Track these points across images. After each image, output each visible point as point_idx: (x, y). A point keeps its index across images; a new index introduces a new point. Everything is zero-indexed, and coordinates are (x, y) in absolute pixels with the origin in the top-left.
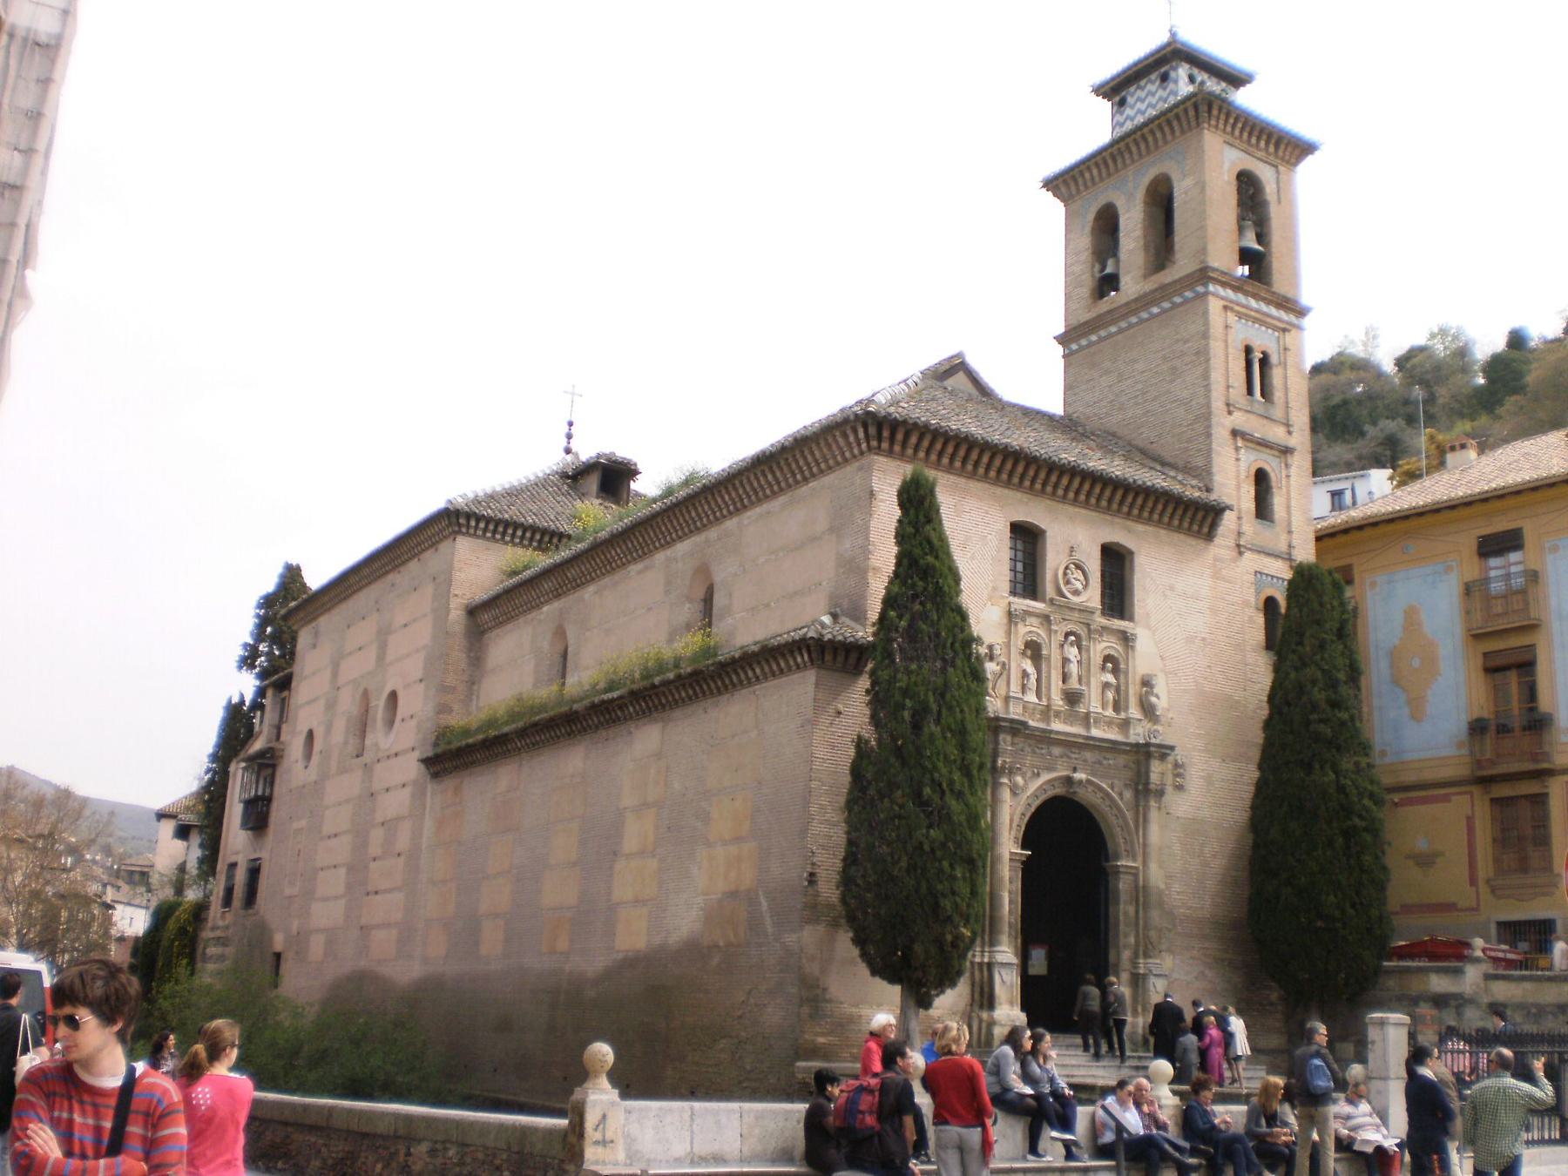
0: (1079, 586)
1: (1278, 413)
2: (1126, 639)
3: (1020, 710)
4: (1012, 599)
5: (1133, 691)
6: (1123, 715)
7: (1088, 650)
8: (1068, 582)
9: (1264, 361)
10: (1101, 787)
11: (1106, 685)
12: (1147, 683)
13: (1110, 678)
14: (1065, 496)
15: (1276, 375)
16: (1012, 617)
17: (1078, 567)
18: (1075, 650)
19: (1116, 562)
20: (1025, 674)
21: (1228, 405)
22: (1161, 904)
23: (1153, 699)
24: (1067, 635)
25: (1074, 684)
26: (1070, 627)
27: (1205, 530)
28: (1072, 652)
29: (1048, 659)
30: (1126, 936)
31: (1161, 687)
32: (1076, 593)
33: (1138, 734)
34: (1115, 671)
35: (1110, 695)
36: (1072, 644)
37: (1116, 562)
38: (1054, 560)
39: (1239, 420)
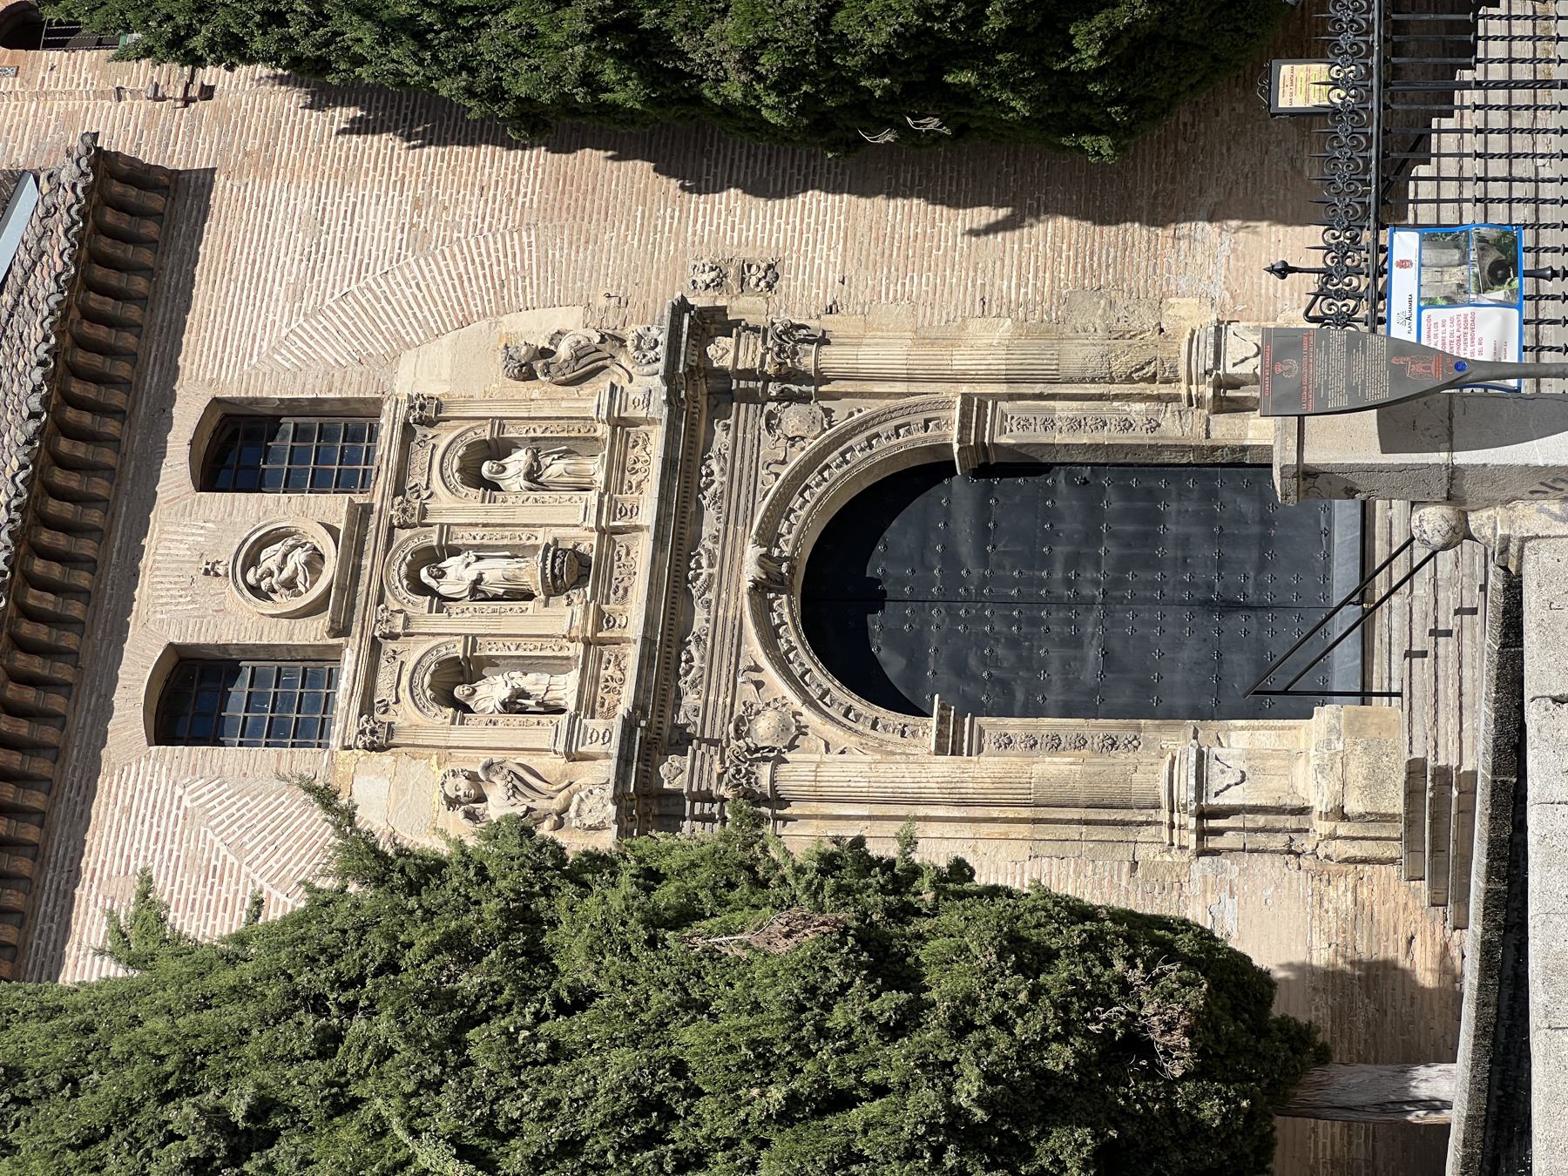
0: (299, 557)
2: (426, 414)
3: (597, 725)
4: (335, 742)
5: (545, 401)
6: (603, 431)
7: (445, 529)
8: (290, 584)
10: (773, 467)
11: (532, 475)
12: (531, 365)
13: (518, 461)
14: (91, 565)
17: (252, 560)
18: (452, 564)
19: (241, 448)
20: (514, 704)
22: (1051, 331)
23: (564, 351)
24: (419, 588)
25: (530, 573)
27: (155, 201)
28: (457, 575)
29: (472, 640)
30: (1127, 425)
31: (532, 328)
32: (315, 560)
33: (643, 386)
34: (498, 449)
35: (555, 469)
37: (241, 448)
38: (235, 621)
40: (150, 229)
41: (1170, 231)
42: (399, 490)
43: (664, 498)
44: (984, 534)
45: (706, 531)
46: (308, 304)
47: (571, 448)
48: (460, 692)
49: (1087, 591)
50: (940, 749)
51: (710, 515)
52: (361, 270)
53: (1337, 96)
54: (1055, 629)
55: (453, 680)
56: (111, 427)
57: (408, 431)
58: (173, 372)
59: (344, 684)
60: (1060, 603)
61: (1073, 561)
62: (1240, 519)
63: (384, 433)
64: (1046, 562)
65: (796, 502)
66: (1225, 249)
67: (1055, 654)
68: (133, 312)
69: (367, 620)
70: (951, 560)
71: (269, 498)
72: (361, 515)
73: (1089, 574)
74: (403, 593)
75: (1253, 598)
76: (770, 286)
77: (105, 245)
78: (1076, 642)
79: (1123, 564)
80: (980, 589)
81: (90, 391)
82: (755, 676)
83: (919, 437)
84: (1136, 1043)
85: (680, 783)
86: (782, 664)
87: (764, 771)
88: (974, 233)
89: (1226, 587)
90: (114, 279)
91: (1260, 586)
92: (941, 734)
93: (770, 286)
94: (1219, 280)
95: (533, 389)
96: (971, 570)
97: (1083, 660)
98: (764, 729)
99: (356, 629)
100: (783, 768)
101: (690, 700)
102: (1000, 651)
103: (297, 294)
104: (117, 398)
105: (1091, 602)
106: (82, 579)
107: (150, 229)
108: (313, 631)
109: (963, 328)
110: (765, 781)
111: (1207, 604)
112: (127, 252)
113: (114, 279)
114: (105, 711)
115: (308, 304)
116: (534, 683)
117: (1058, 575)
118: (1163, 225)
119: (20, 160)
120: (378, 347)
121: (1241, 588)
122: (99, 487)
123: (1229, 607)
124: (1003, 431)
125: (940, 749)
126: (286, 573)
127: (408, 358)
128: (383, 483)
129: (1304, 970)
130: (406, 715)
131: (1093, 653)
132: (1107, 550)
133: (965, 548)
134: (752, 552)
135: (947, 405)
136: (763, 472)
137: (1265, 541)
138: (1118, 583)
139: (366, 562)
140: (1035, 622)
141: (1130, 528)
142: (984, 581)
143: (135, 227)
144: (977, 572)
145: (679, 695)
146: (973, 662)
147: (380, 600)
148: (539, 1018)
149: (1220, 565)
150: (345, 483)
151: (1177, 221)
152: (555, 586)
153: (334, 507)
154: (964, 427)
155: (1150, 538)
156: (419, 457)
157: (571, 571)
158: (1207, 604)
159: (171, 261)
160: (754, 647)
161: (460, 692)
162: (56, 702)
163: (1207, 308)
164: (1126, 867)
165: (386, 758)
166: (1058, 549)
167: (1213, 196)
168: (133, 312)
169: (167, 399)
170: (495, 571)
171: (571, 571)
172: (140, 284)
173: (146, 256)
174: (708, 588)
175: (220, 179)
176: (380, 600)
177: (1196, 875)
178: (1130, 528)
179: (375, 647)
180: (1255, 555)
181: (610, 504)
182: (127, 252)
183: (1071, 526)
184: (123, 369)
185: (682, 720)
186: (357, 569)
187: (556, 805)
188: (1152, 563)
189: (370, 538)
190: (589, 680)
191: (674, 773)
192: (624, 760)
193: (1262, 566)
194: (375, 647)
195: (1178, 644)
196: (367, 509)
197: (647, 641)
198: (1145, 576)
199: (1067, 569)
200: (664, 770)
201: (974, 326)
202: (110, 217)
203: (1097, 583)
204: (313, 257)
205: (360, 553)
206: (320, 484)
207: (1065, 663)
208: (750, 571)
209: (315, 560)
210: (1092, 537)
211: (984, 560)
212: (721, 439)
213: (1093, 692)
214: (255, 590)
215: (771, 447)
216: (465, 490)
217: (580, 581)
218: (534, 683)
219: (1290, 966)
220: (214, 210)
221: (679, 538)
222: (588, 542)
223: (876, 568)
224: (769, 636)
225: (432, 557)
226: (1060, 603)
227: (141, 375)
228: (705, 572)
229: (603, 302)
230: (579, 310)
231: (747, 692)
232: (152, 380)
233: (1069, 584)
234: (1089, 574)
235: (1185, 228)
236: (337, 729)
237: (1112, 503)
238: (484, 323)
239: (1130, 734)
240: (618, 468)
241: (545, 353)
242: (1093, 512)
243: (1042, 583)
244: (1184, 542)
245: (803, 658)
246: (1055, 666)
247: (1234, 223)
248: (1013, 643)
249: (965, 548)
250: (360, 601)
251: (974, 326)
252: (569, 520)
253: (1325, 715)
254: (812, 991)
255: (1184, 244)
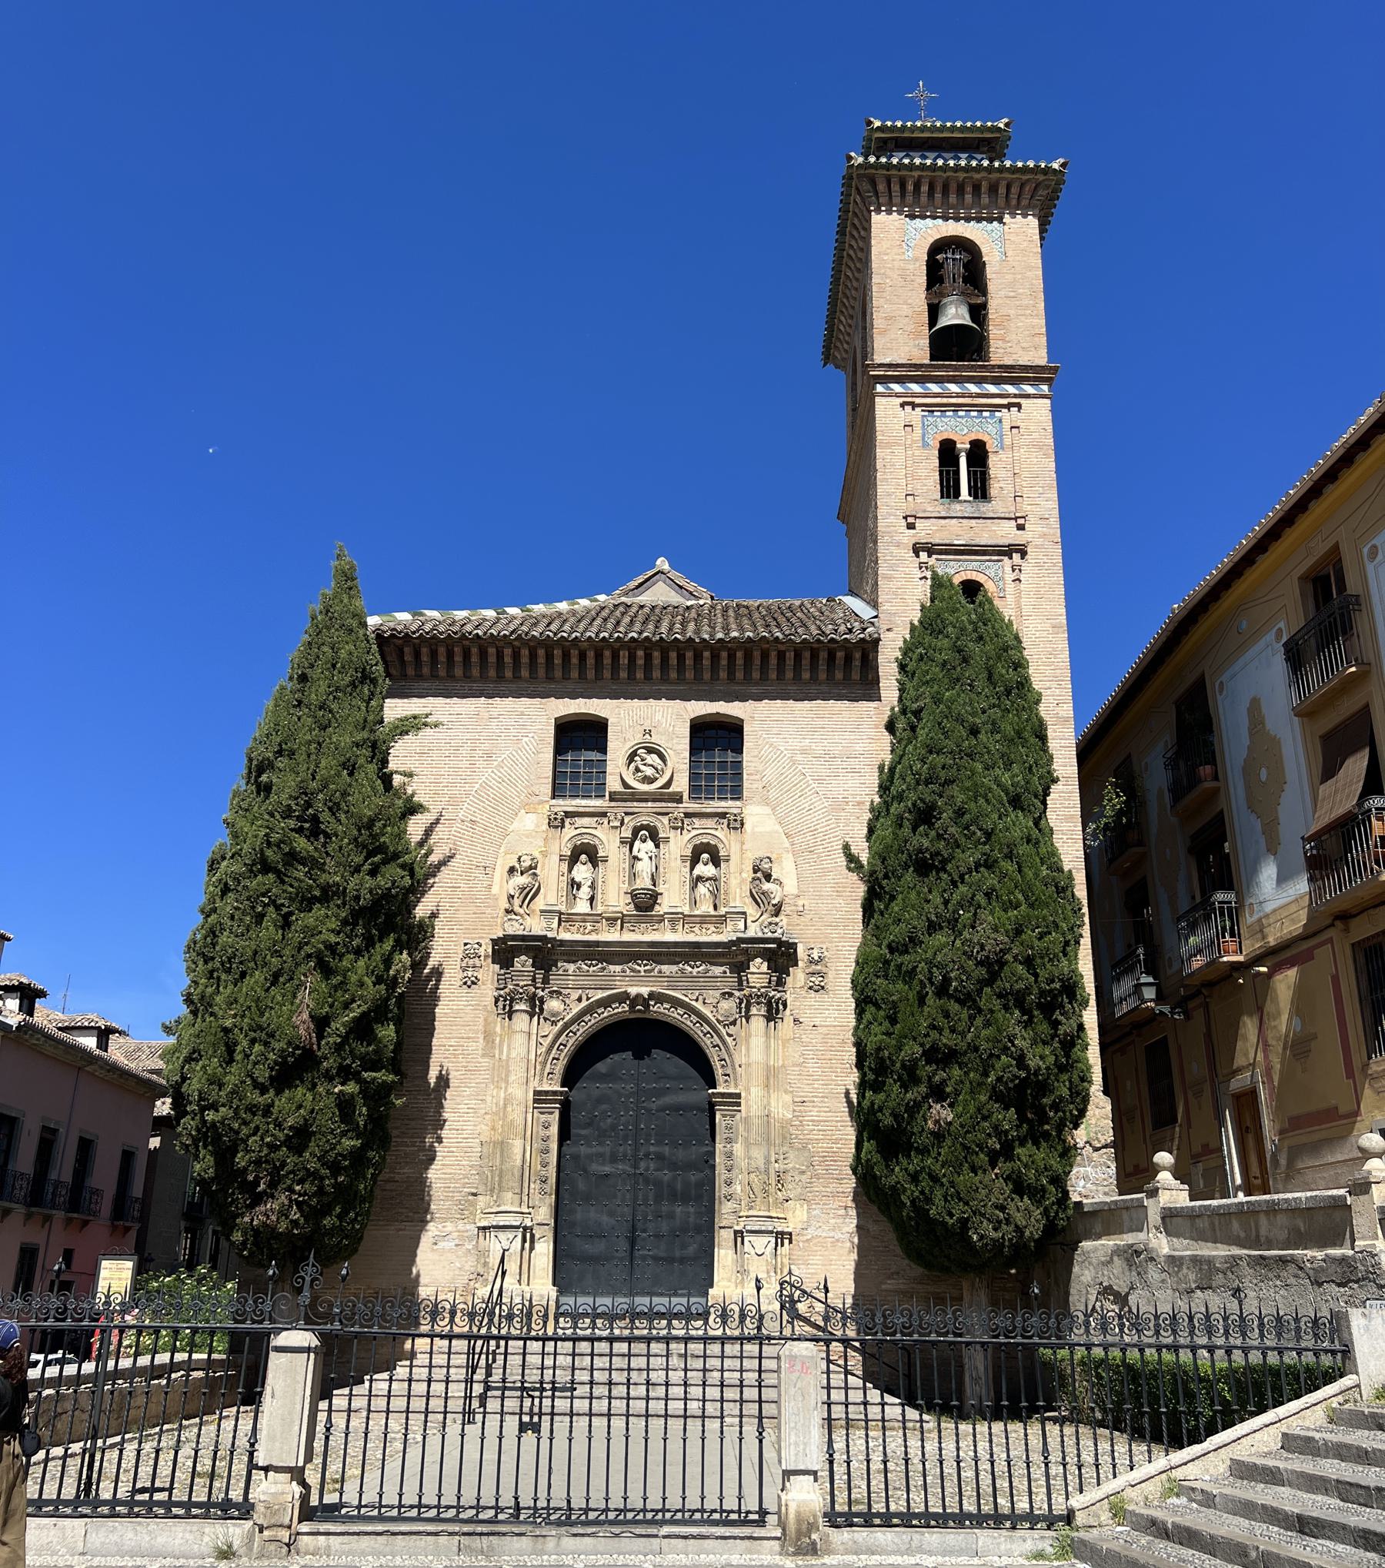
0: (649, 772)
1: (999, 504)
2: (737, 824)
8: (637, 770)
9: (978, 453)
13: (709, 870)
15: (997, 466)
16: (557, 823)
17: (650, 751)
18: (650, 844)
21: (905, 518)
24: (636, 831)
26: (644, 820)
27: (856, 675)
30: (729, 1183)
31: (785, 870)
32: (650, 780)
34: (716, 861)
36: (644, 841)
39: (926, 531)
40: (839, 675)
41: (851, 1204)
42: (687, 815)
43: (676, 944)
44: (676, 1108)
45: (665, 968)
46: (799, 757)
47: (715, 895)
48: (583, 857)
49: (642, 1165)
50: (536, 1093)
51: (674, 968)
52: (819, 780)
53: (101, 1297)
54: (621, 1149)
55: (586, 852)
56: (723, 675)
57: (723, 815)
58: (758, 698)
59: (584, 802)
60: (636, 1150)
61: (660, 1157)
62: (684, 1247)
63: (723, 804)
64: (659, 1143)
65: (681, 1011)
66: (838, 1235)
67: (607, 1149)
68: (789, 675)
69: (619, 808)
70: (660, 1093)
71: (687, 754)
72: (677, 798)
73: (652, 1166)
74: (632, 824)
75: (637, 1254)
76: (811, 988)
77: (823, 655)
78: (614, 1159)
79: (658, 1184)
80: (644, 1108)
81: (740, 661)
82: (584, 997)
83: (719, 1072)
84: (258, 1199)
85: (517, 966)
86: (589, 1010)
87: (523, 1006)
88: (847, 1093)
89: (644, 1239)
90: (806, 662)
91: (644, 1258)
92: (547, 1093)
93: (811, 988)
94: (819, 1232)
95: (748, 875)
96: (655, 1104)
97: (603, 1164)
98: (553, 1005)
99: (613, 804)
100: (526, 1017)
101: (571, 967)
102: (609, 1120)
103: (803, 752)
104: (739, 675)
105: (636, 1167)
106: (640, 675)
107: (839, 675)
108: (613, 784)
109: (786, 1092)
110: (517, 1007)
111: (634, 1229)
112: (822, 666)
113: (806, 662)
114: (573, 696)
115: (799, 757)
116: (585, 892)
117: (652, 1149)
118: (854, 1200)
119: (885, 607)
120: (773, 794)
121: (643, 1248)
122: (690, 675)
123: (633, 1242)
124: (724, 1116)
125: (536, 1093)
126: (642, 768)
127: (768, 810)
128: (694, 807)
129: (416, 1282)
130: (569, 832)
131: (607, 1169)
132: (666, 1175)
133: (668, 1100)
134: (644, 991)
135: (736, 1086)
136: (697, 993)
137: (670, 1260)
138: (647, 1181)
139: (650, 804)
140: (626, 1138)
141: (679, 1187)
142: (649, 1110)
143: (836, 667)
144: (654, 1106)
145: (574, 962)
146: (604, 1107)
147: (627, 814)
148: (278, 908)
149: (656, 1236)
150: (695, 790)
151: (857, 1208)
152: (634, 895)
153: (681, 784)
154: (723, 1095)
155: (674, 1196)
156: (710, 823)
157: (645, 903)
158: (634, 1229)
159: (824, 688)
160: (600, 995)
161: (583, 857)
162: (690, 675)
163: (800, 1226)
164: (474, 1191)
165: (545, 827)
166: (667, 1148)
167: (874, 1228)
168: (789, 675)
169: (743, 698)
170: (644, 867)
171: (645, 903)
172: (806, 675)
173: (823, 676)
174: (633, 970)
175: (875, 704)
176: (627, 814)
177: (468, 1227)
178: (679, 1187)
179: (604, 815)
180: (662, 1254)
181: (685, 918)
182: (822, 666)
183: (681, 1154)
184: (756, 675)
185: (559, 964)
186: (646, 801)
187: (517, 909)
188: (658, 1199)
189: (664, 804)
190: (584, 918)
191: (523, 963)
192: (523, 938)
193: (656, 1258)
194: (604, 815)
195: (611, 1214)
196: (680, 800)
197: (597, 943)
198: (651, 1195)
199: (655, 1153)
200: (523, 958)
201: (788, 1098)
202: (840, 654)
203: (647, 1169)
204: (828, 757)
205: (654, 800)
206: (693, 776)
207: (601, 1155)
208: (633, 991)
209: (650, 780)
210: (674, 1166)
211: (662, 1109)
212: (717, 970)
213: (585, 1171)
214: (634, 754)
215: (713, 996)
216: (690, 847)
217: (638, 908)
218: (585, 892)
219: (418, 1275)
220: (856, 704)
221: (659, 954)
222: (663, 907)
223: (656, 1053)
224: (605, 1003)
225: (654, 835)
226: (636, 1150)
227: (757, 684)
228: (642, 969)
229: (800, 903)
230: (796, 892)
231: (575, 995)
232: (754, 690)
233: (647, 1155)
234: (652, 1166)
235: (853, 1213)
236: (561, 802)
237: (694, 1177)
238: (787, 845)
239: (548, 1190)
240: (704, 920)
241: (768, 877)
242: (690, 1166)
243: (647, 1140)
244: (671, 1216)
245: (592, 1022)
246: (600, 1149)
247: (856, 1240)
248: (614, 1128)
249: (668, 1100)
250: (629, 804)
251: (788, 1098)
252: (673, 897)
253: (553, 1292)
254: (272, 1035)
255: (842, 1212)
